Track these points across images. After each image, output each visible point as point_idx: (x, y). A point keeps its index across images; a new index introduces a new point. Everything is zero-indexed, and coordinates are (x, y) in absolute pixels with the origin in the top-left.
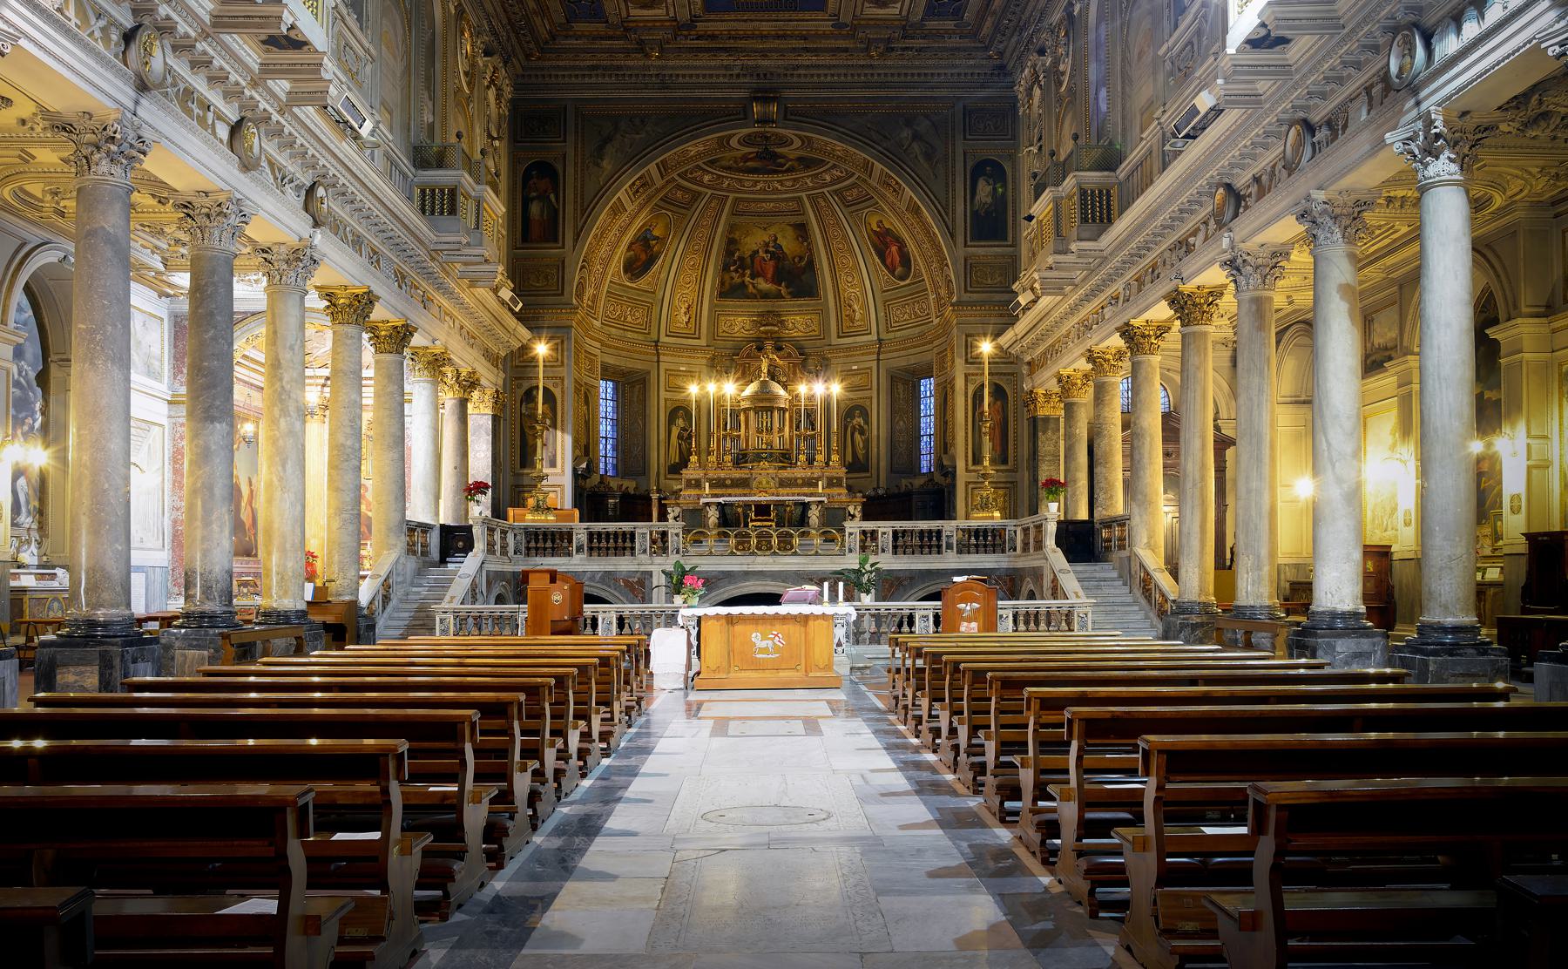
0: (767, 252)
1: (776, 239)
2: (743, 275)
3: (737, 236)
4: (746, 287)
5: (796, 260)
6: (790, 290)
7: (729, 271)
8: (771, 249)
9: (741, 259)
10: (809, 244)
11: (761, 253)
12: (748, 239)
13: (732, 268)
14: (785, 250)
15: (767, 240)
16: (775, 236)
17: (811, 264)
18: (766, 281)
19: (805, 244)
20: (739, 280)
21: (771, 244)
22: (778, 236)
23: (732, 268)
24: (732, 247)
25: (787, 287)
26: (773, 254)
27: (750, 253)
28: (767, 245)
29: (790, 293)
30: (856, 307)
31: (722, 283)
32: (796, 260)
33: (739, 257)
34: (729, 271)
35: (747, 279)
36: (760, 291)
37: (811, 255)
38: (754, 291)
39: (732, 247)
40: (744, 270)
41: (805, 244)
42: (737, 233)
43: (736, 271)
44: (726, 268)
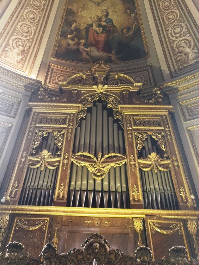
0: (99, 26)
1: (108, 14)
2: (79, 44)
3: (74, 8)
4: (81, 53)
5: (125, 31)
6: (118, 56)
7: (66, 38)
8: (103, 24)
9: (78, 30)
10: (136, 14)
11: (95, 27)
12: (84, 14)
13: (69, 36)
14: (114, 22)
15: (100, 15)
16: (107, 10)
17: (138, 33)
18: (98, 50)
19: (133, 15)
20: (75, 47)
21: (104, 19)
22: (110, 11)
23: (69, 36)
24: (70, 18)
25: (116, 54)
26: (104, 27)
27: (85, 26)
28: (100, 19)
29: (119, 59)
30: (188, 50)
31: (60, 46)
32: (125, 31)
33: (75, 28)
34: (66, 38)
35: (82, 47)
36: (92, 57)
37: (138, 24)
38: (88, 57)
39: (70, 18)
40: (79, 38)
41: (133, 15)
42: (75, 5)
43: (72, 39)
44: (63, 35)
